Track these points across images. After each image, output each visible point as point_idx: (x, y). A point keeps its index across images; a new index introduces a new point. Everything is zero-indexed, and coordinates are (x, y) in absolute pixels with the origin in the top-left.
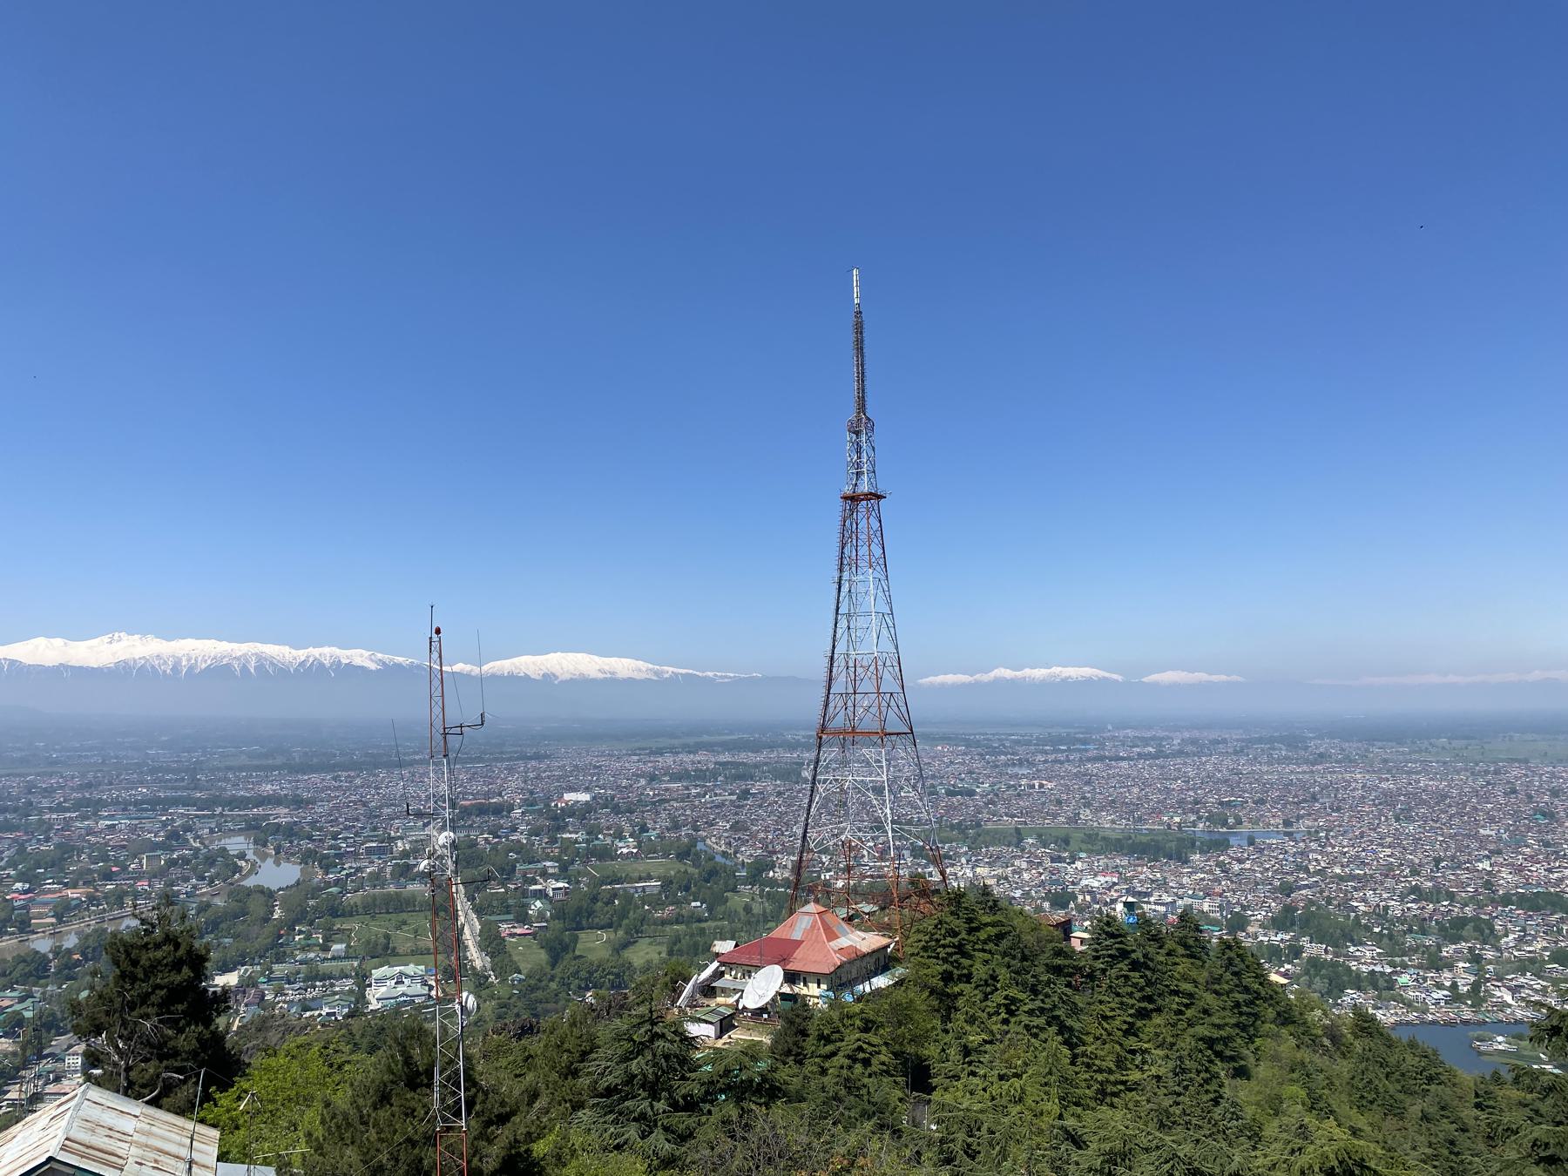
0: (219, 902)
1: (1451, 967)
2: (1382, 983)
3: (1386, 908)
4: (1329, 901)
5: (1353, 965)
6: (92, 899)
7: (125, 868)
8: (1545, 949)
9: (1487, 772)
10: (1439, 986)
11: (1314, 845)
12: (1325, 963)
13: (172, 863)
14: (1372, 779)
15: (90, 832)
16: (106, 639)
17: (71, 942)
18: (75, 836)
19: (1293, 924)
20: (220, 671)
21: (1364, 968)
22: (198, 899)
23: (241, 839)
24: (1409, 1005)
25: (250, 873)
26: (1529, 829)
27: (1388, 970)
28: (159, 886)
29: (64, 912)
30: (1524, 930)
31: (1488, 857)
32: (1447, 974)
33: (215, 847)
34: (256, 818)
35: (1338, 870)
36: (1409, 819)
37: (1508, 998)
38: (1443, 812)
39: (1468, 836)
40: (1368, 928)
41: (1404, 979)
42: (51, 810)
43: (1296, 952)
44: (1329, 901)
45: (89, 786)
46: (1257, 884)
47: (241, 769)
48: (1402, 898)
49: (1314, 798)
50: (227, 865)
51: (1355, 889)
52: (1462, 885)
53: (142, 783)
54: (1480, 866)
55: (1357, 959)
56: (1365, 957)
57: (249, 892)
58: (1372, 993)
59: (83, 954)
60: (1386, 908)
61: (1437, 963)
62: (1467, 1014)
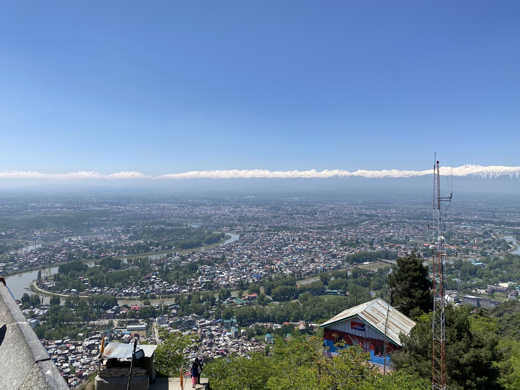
0: (502, 258)
6: (458, 250)
7: (469, 242)
13: (485, 242)
15: (458, 229)
16: (464, 167)
17: (452, 263)
18: (453, 230)
20: (504, 177)
22: (494, 256)
23: (511, 237)
25: (514, 249)
28: (480, 249)
29: (450, 253)
33: (501, 239)
34: (517, 230)
42: (447, 221)
45: (458, 214)
47: (512, 212)
50: (505, 246)
53: (475, 215)
57: (513, 256)
59: (455, 267)
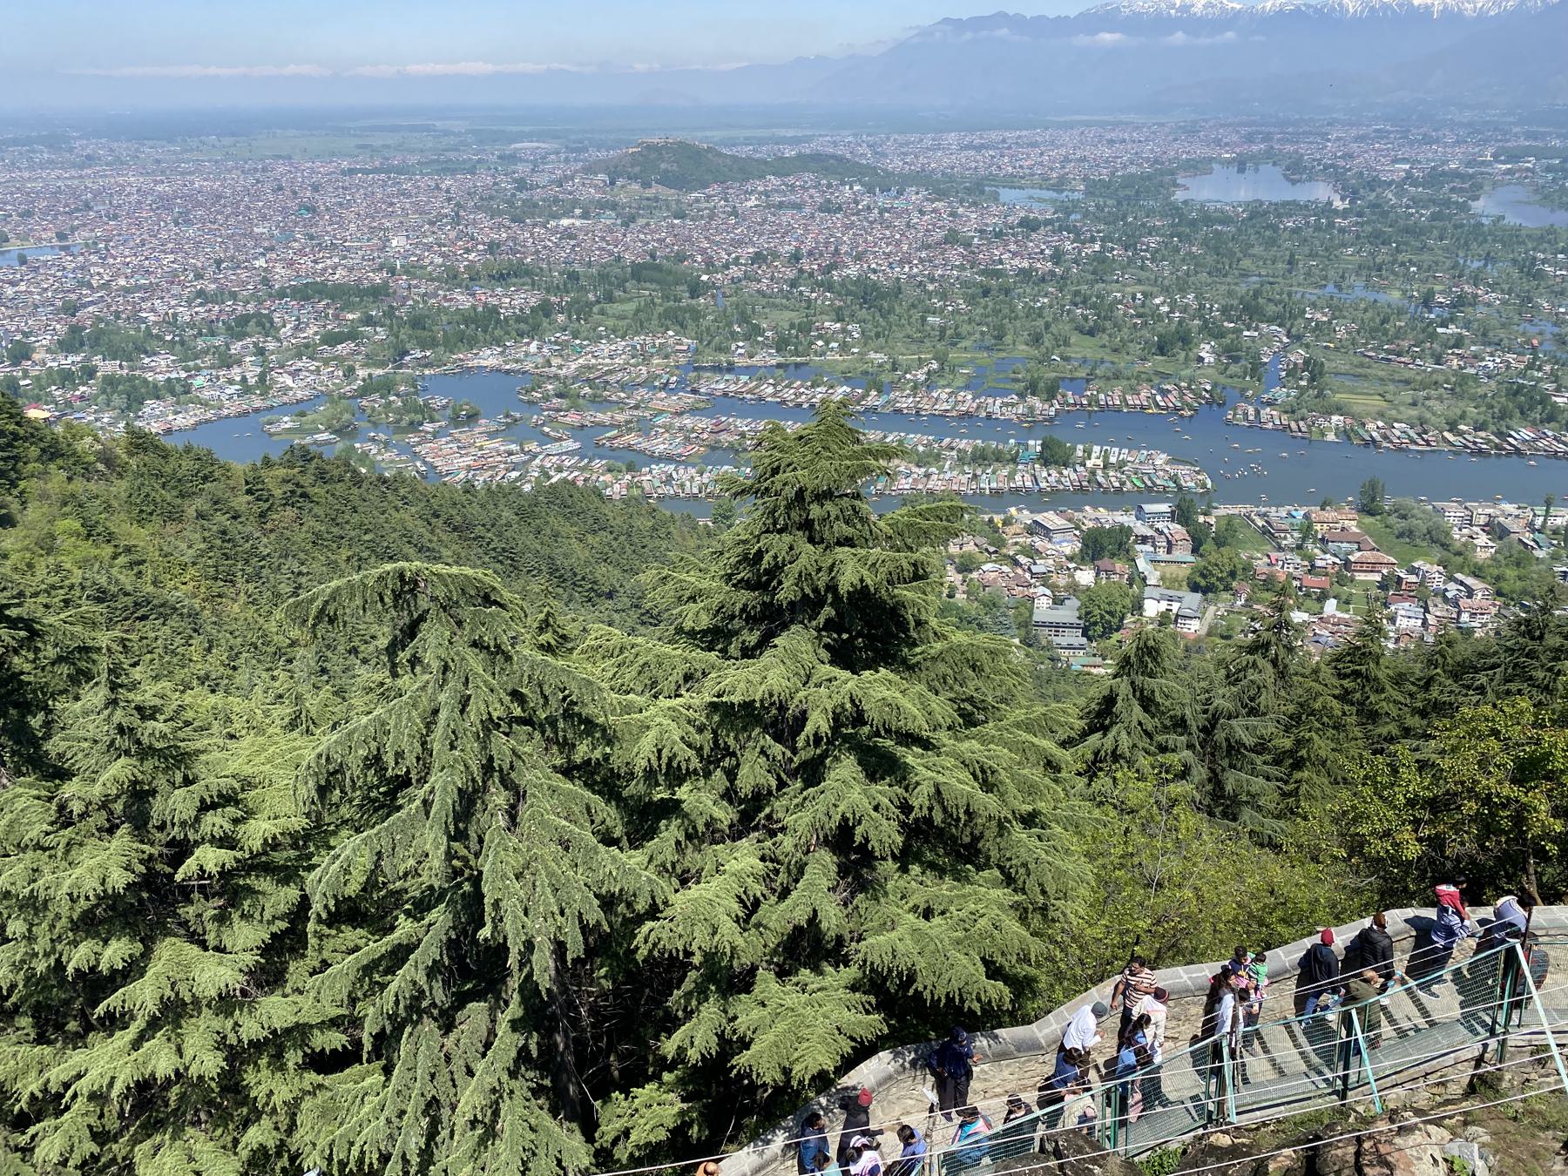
1: (239, 363)
2: (178, 388)
3: (175, 315)
4: (118, 318)
5: (149, 376)
8: (316, 333)
9: (256, 170)
10: (231, 382)
11: (94, 258)
12: (121, 380)
14: (145, 182)
19: (82, 344)
21: (160, 377)
24: (205, 404)
26: (296, 224)
27: (183, 375)
30: (298, 319)
31: (264, 255)
32: (236, 370)
35: (122, 282)
36: (188, 222)
37: (289, 382)
38: (219, 213)
39: (244, 235)
40: (159, 338)
41: (199, 381)
43: (90, 372)
44: (117, 315)
46: (36, 307)
48: (189, 303)
49: (88, 207)
51: (143, 300)
52: (244, 284)
54: (257, 264)
55: (152, 369)
56: (161, 367)
58: (171, 399)
60: (175, 315)
61: (227, 362)
62: (258, 403)
